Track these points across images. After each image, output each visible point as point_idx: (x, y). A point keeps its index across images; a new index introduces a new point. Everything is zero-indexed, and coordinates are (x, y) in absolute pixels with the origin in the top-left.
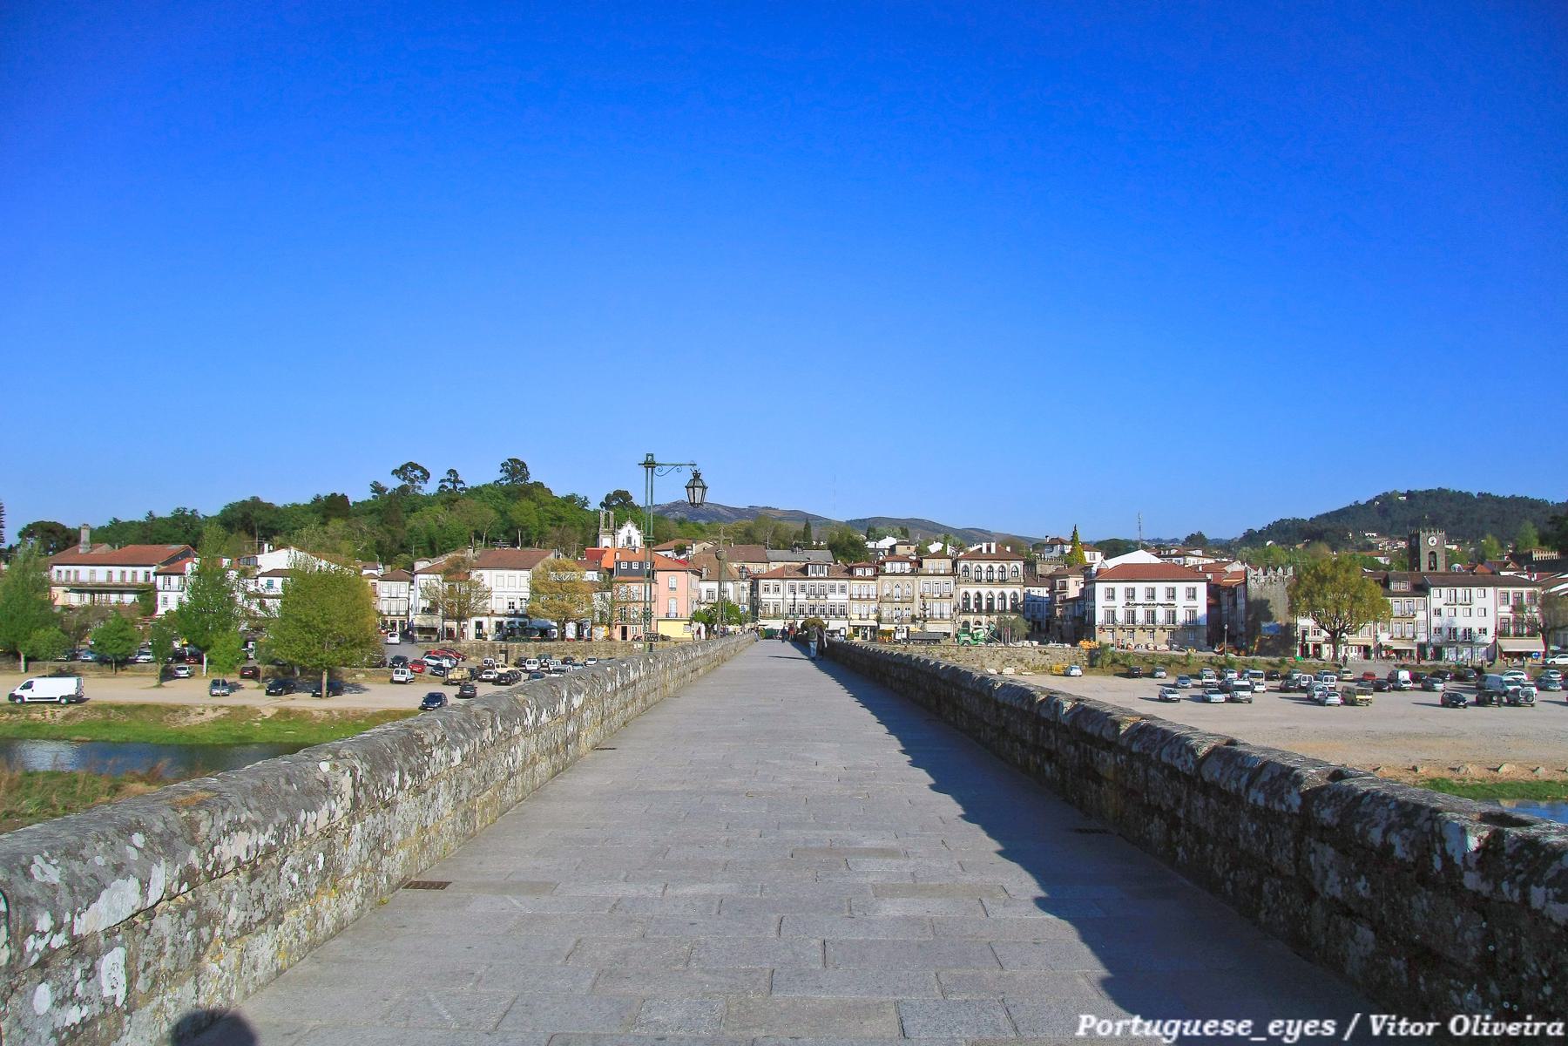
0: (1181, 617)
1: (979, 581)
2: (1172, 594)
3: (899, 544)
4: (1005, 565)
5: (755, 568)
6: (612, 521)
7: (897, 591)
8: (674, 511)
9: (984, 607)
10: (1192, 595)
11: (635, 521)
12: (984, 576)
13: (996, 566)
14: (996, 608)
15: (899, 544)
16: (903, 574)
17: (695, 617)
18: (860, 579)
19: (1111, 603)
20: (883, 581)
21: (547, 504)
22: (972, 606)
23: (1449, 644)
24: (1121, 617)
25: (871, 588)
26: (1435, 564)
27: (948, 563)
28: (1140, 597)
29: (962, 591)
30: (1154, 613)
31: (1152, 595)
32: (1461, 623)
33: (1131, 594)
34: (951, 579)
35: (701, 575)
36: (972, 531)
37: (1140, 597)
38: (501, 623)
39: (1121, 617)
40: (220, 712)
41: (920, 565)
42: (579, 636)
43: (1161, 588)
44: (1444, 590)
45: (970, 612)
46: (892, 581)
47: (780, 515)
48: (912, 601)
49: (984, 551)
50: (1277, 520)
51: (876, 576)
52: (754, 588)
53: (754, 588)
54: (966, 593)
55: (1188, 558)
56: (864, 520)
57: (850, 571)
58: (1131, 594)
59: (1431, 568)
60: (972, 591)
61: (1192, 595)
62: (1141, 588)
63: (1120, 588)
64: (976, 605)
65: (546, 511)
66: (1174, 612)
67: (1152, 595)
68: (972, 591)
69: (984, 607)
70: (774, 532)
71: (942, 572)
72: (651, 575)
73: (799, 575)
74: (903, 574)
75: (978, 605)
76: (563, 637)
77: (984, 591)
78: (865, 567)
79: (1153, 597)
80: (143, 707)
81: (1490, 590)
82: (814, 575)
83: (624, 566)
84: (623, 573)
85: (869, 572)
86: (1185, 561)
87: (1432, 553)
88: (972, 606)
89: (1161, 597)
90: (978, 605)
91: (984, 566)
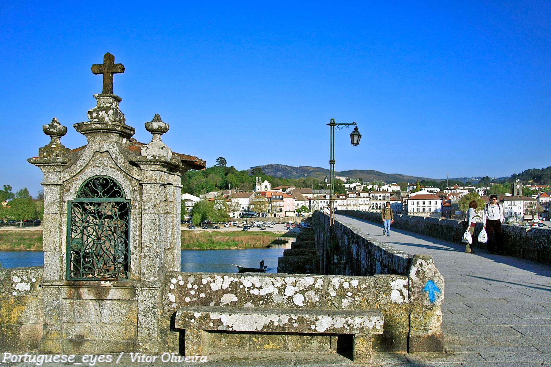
0: (433, 210)
1: (377, 199)
2: (430, 203)
3: (357, 186)
4: (385, 195)
5: (310, 196)
6: (260, 180)
7: (352, 203)
8: (267, 168)
9: (378, 207)
10: (436, 203)
11: (268, 180)
12: (378, 198)
13: (382, 195)
14: (382, 207)
15: (357, 186)
16: (354, 198)
17: (296, 211)
18: (341, 199)
19: (413, 206)
20: (348, 200)
21: (238, 175)
22: (375, 207)
23: (510, 217)
24: (415, 210)
25: (345, 202)
26: (519, 193)
27: (367, 194)
28: (421, 204)
29: (372, 202)
30: (425, 208)
31: (424, 203)
32: (514, 210)
33: (418, 203)
34: (368, 199)
35: (295, 199)
36: (396, 175)
37: (421, 204)
38: (240, 213)
39: (415, 210)
40: (200, 232)
41: (359, 195)
42: (263, 217)
43: (427, 202)
44: (508, 201)
45: (375, 209)
46: (351, 200)
47: (312, 169)
48: (357, 206)
49: (378, 190)
50: (526, 169)
51: (346, 198)
52: (310, 202)
53: (310, 202)
54: (373, 203)
55: (457, 190)
56: (349, 171)
57: (338, 197)
58: (418, 203)
59: (517, 195)
60: (375, 202)
61: (436, 203)
62: (421, 202)
63: (415, 202)
64: (376, 207)
65: (238, 177)
66: (431, 208)
67: (424, 203)
68: (375, 202)
69: (378, 207)
70: (313, 182)
71: (366, 197)
72: (282, 199)
73: (323, 198)
74: (354, 198)
75: (377, 207)
76: (258, 217)
77: (378, 202)
78: (343, 196)
79: (425, 204)
80: (185, 230)
81: (522, 201)
82: (327, 198)
83: (274, 197)
84: (274, 199)
85: (344, 197)
86: (456, 191)
87: (518, 190)
88: (375, 207)
89: (427, 204)
90: (377, 207)
91: (378, 195)
